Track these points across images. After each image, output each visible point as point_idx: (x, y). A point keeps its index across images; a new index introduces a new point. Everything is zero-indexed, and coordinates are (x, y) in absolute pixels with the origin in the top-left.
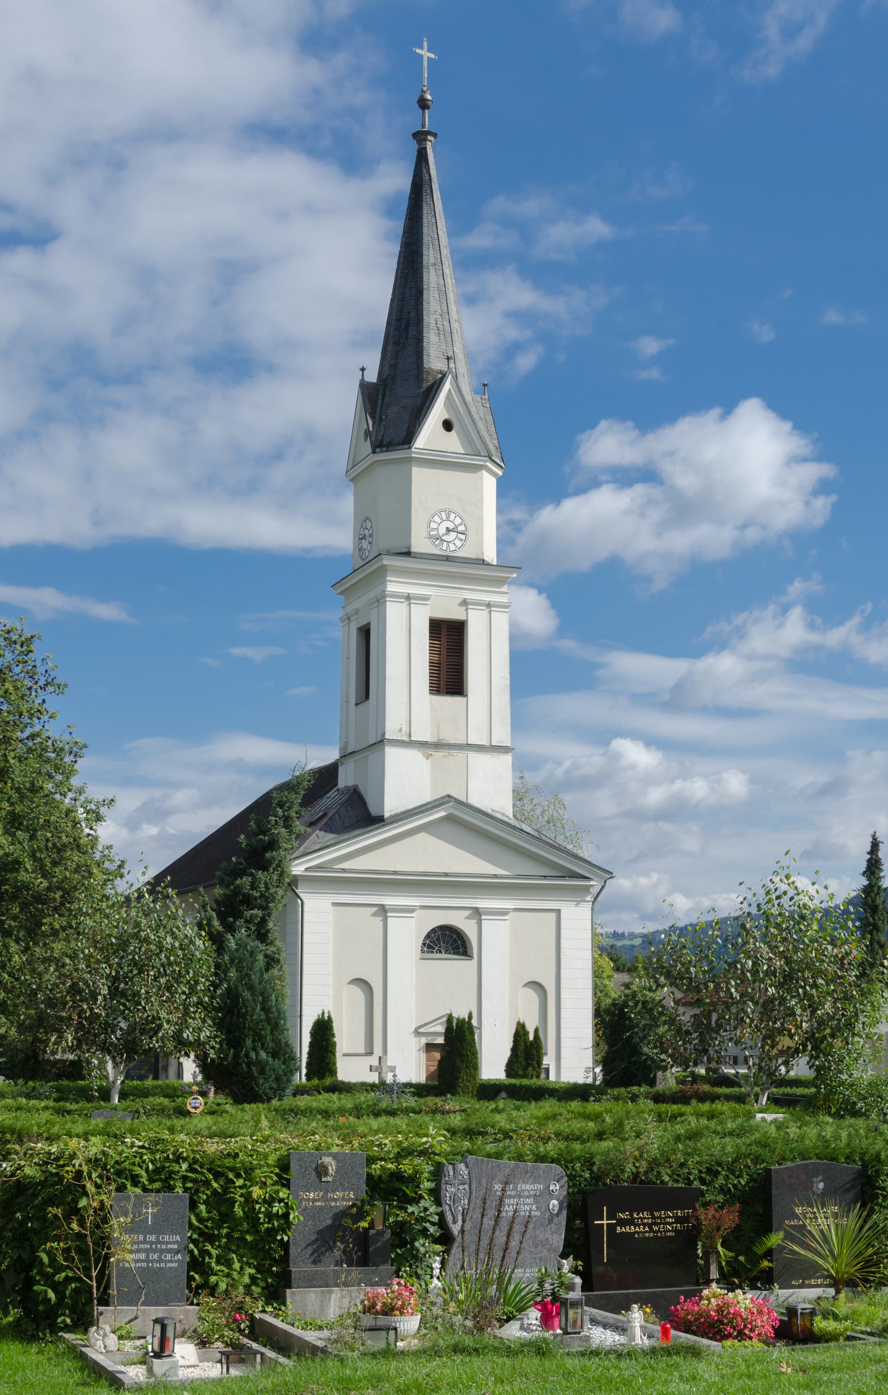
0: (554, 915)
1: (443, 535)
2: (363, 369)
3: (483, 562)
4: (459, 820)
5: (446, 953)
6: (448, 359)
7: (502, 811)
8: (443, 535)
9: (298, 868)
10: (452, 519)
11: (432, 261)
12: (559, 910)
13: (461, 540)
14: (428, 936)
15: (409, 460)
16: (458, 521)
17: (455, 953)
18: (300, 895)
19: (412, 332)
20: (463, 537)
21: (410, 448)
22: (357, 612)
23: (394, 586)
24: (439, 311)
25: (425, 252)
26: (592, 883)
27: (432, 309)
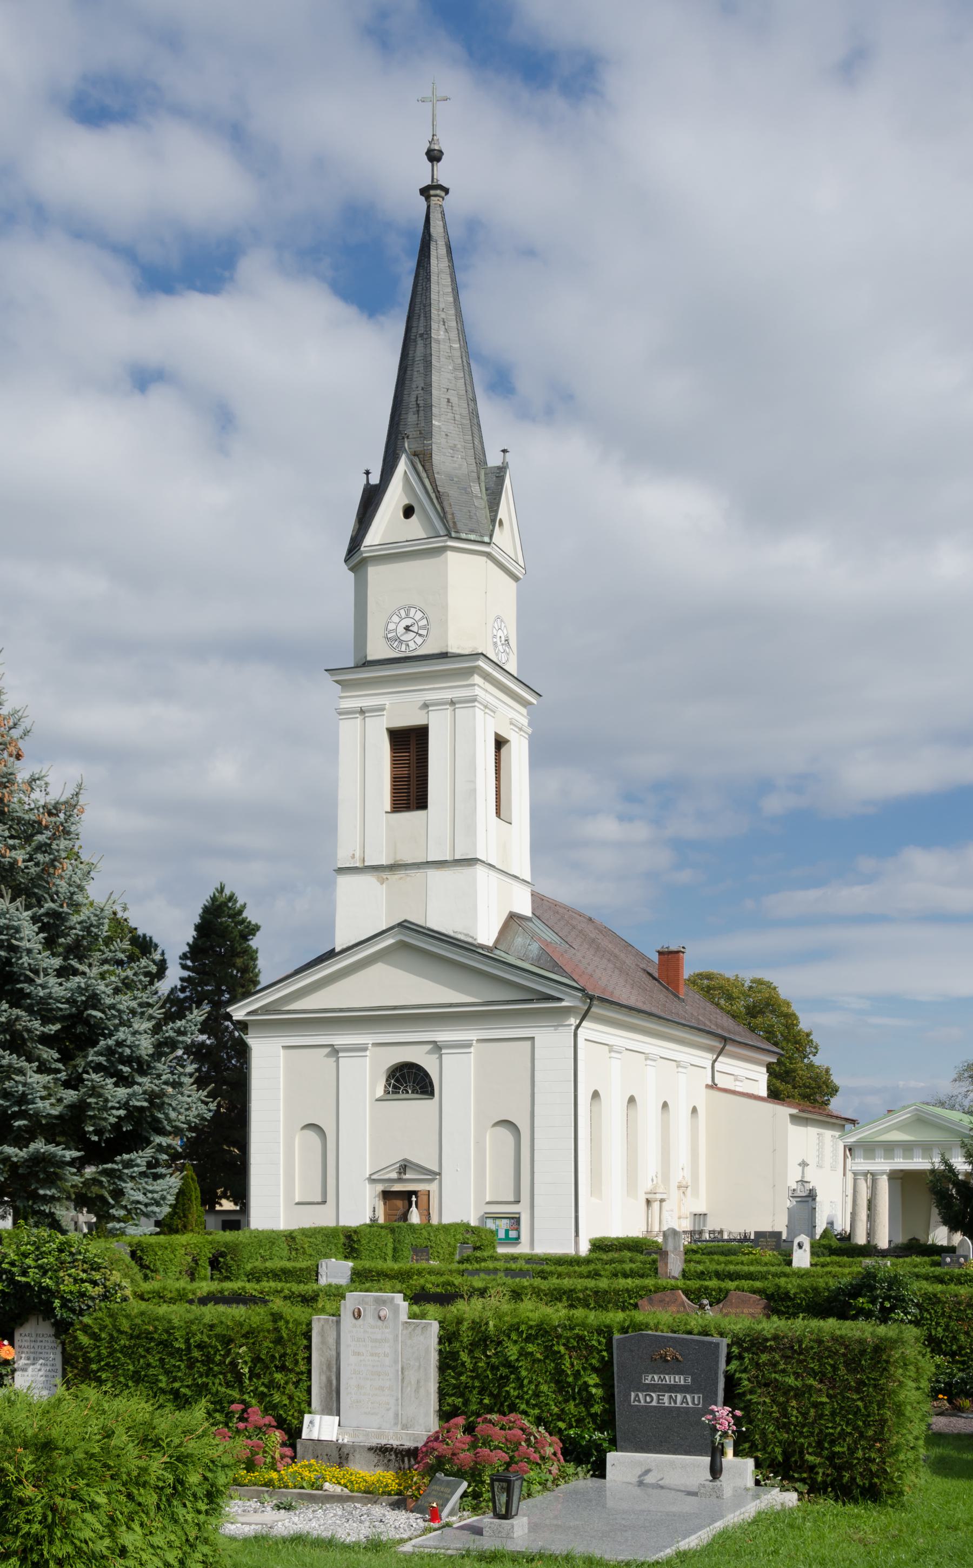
0: (528, 1044)
3: (444, 656)
4: (417, 943)
5: (413, 1092)
7: (465, 932)
10: (411, 615)
11: (421, 330)
12: (533, 1038)
15: (364, 562)
17: (422, 1093)
24: (422, 385)
26: (564, 1004)
27: (414, 386)
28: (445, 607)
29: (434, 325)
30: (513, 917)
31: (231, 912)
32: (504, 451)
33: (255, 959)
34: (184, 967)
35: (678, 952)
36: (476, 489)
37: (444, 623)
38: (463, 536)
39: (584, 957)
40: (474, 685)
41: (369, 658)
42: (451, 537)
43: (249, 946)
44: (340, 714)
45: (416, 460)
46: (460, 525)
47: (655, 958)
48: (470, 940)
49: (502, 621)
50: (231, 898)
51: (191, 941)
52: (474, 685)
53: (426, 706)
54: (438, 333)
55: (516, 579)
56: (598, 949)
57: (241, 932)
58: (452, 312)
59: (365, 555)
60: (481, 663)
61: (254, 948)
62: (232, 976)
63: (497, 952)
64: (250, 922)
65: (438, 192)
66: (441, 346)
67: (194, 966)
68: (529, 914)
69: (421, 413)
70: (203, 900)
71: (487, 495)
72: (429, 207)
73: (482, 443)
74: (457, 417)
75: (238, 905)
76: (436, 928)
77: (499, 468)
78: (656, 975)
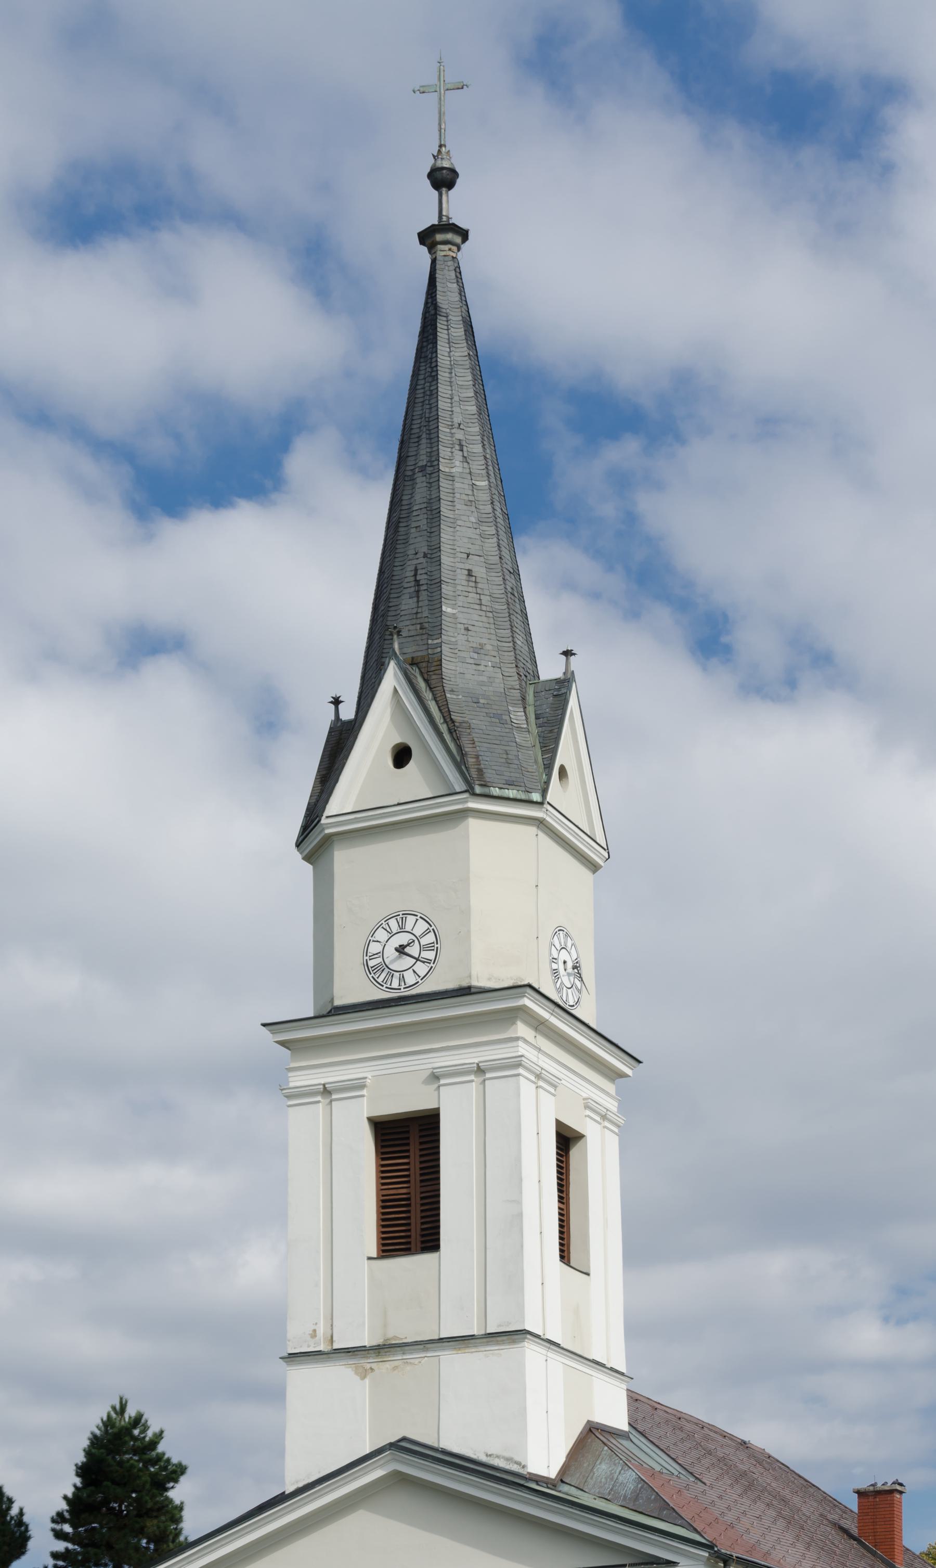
1: (393, 961)
3: (465, 991)
7: (507, 1455)
8: (393, 961)
10: (408, 928)
11: (423, 460)
15: (328, 841)
16: (422, 926)
24: (425, 549)
28: (466, 913)
29: (444, 452)
30: (593, 1433)
31: (138, 1444)
32: (568, 653)
33: (178, 1520)
34: (59, 1535)
35: (891, 1492)
36: (518, 716)
37: (464, 938)
38: (496, 791)
39: (720, 1497)
40: (517, 1039)
41: (338, 1002)
42: (474, 794)
43: (167, 1498)
44: (289, 1097)
45: (415, 672)
46: (489, 775)
47: (853, 1503)
48: (515, 1468)
49: (567, 935)
50: (137, 1421)
51: (70, 1492)
52: (517, 1039)
53: (435, 1077)
54: (451, 464)
55: (594, 867)
56: (750, 1486)
57: (153, 1476)
58: (476, 429)
59: (327, 831)
60: (528, 1002)
61: (177, 1502)
62: (137, 1548)
63: (565, 1488)
64: (168, 1460)
65: (449, 236)
66: (457, 485)
67: (76, 1533)
68: (625, 1427)
69: (424, 595)
70: (89, 1420)
71: (538, 726)
72: (434, 262)
73: (530, 643)
74: (485, 600)
75: (150, 1434)
76: (456, 1450)
77: (558, 681)
78: (855, 1531)
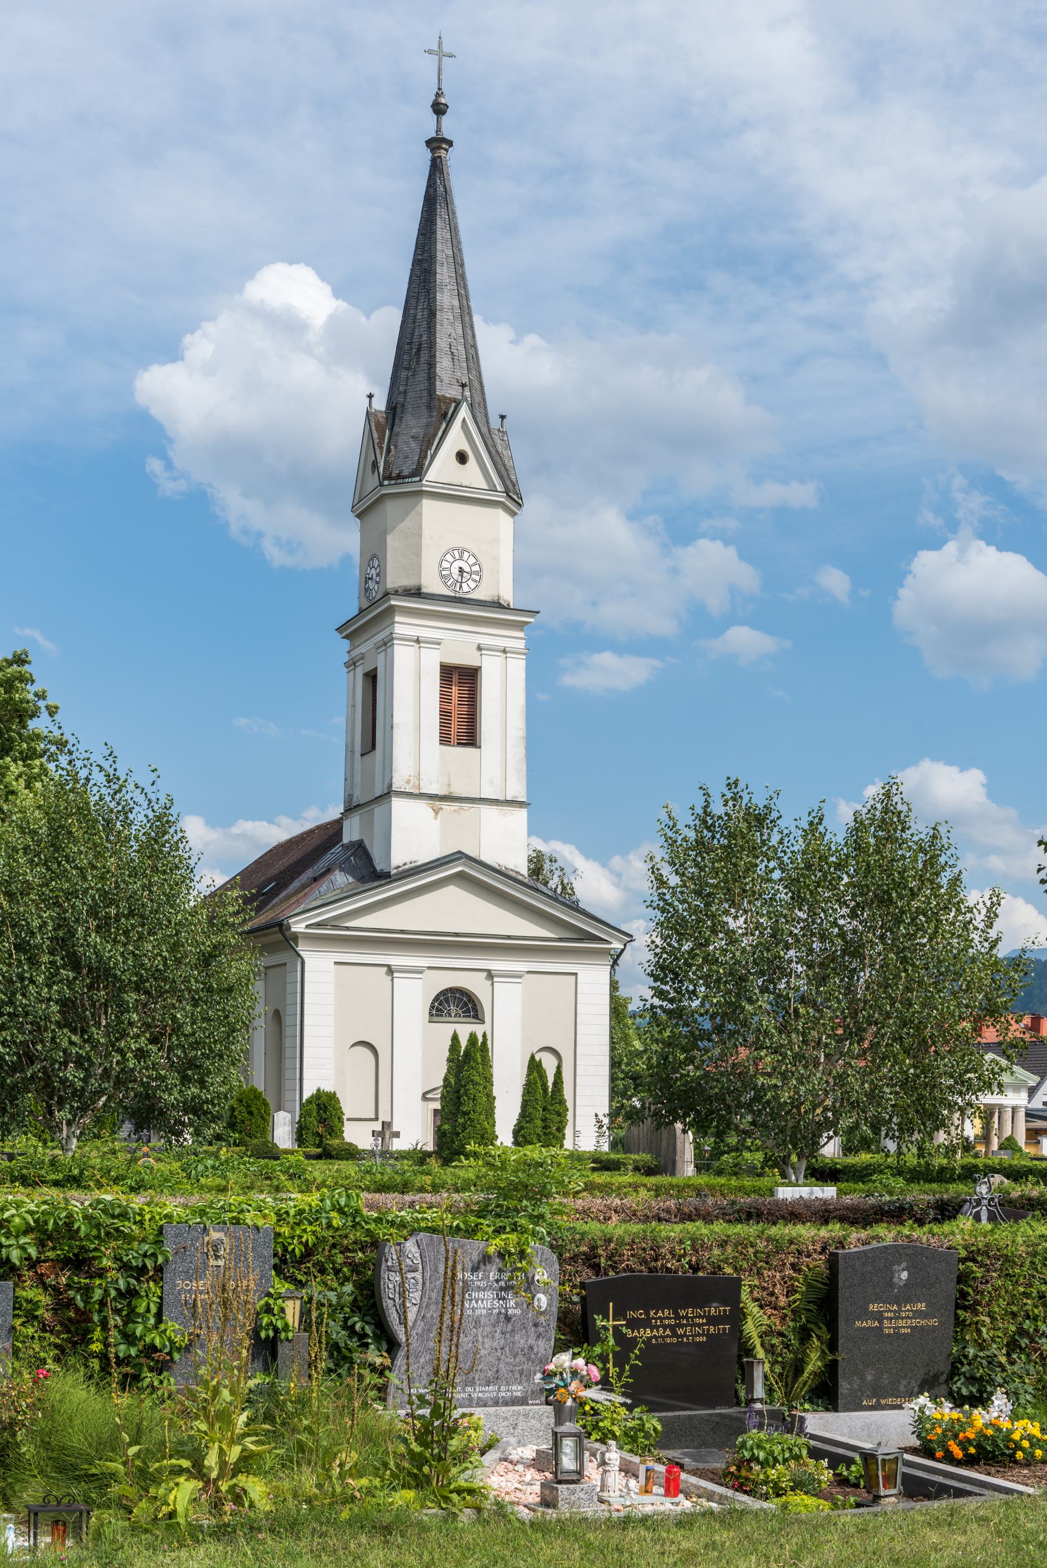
2: (370, 396)
5: (455, 1016)
6: (463, 386)
9: (298, 926)
13: (475, 581)
14: (436, 999)
15: (420, 494)
16: (472, 560)
18: (301, 953)
19: (424, 357)
20: (477, 578)
21: (421, 480)
22: (362, 657)
23: (403, 626)
25: (438, 270)
